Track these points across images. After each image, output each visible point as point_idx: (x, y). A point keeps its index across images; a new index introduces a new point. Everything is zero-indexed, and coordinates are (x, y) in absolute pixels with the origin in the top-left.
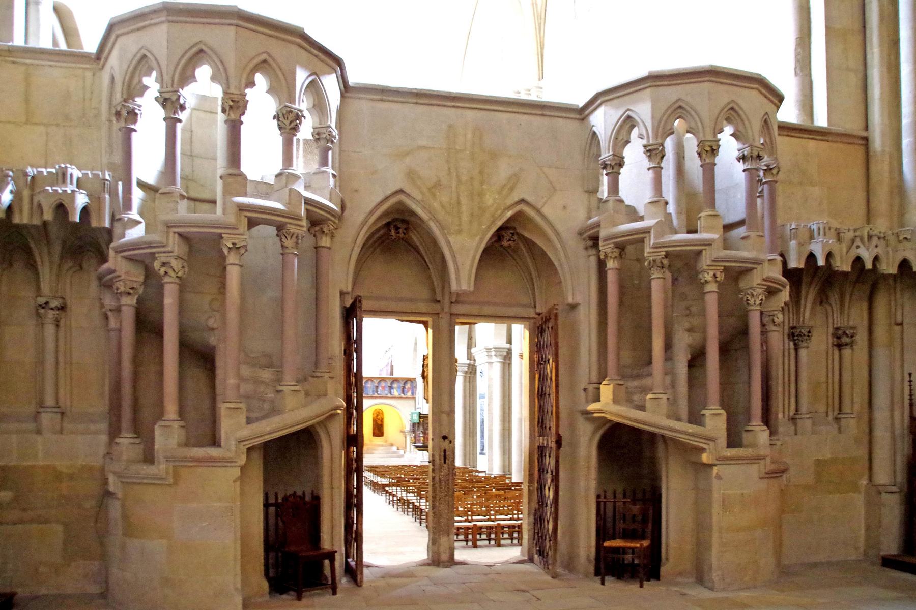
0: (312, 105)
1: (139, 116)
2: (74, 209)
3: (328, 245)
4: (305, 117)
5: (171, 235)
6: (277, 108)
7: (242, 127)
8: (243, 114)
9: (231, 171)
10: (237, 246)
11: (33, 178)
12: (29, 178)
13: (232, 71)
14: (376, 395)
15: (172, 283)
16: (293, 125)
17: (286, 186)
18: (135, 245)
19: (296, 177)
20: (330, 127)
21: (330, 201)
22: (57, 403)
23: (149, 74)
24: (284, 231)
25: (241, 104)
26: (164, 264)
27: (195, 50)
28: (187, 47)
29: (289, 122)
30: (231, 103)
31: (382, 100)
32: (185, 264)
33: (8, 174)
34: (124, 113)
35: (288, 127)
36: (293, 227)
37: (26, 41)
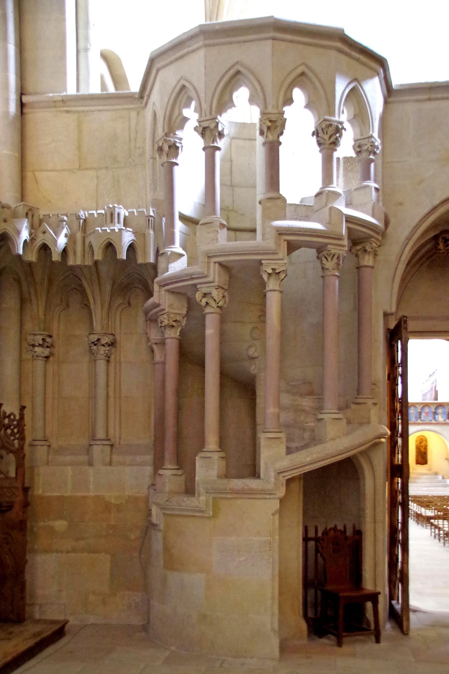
0: (352, 117)
1: (180, 149)
2: (121, 247)
4: (345, 129)
5: (212, 265)
6: (316, 123)
7: (281, 148)
8: (282, 133)
9: (270, 195)
10: (277, 271)
11: (85, 220)
12: (82, 221)
13: (269, 89)
14: (419, 421)
15: (212, 313)
16: (332, 139)
17: (326, 205)
18: (177, 278)
19: (336, 195)
20: (372, 137)
21: (373, 216)
22: (107, 436)
23: (188, 105)
24: (325, 253)
25: (279, 123)
26: (205, 295)
27: (232, 72)
28: (224, 70)
29: (328, 136)
30: (269, 124)
31: (430, 99)
32: (226, 293)
33: (63, 218)
34: (166, 148)
35: (328, 142)
36: (334, 247)
37: (78, 90)
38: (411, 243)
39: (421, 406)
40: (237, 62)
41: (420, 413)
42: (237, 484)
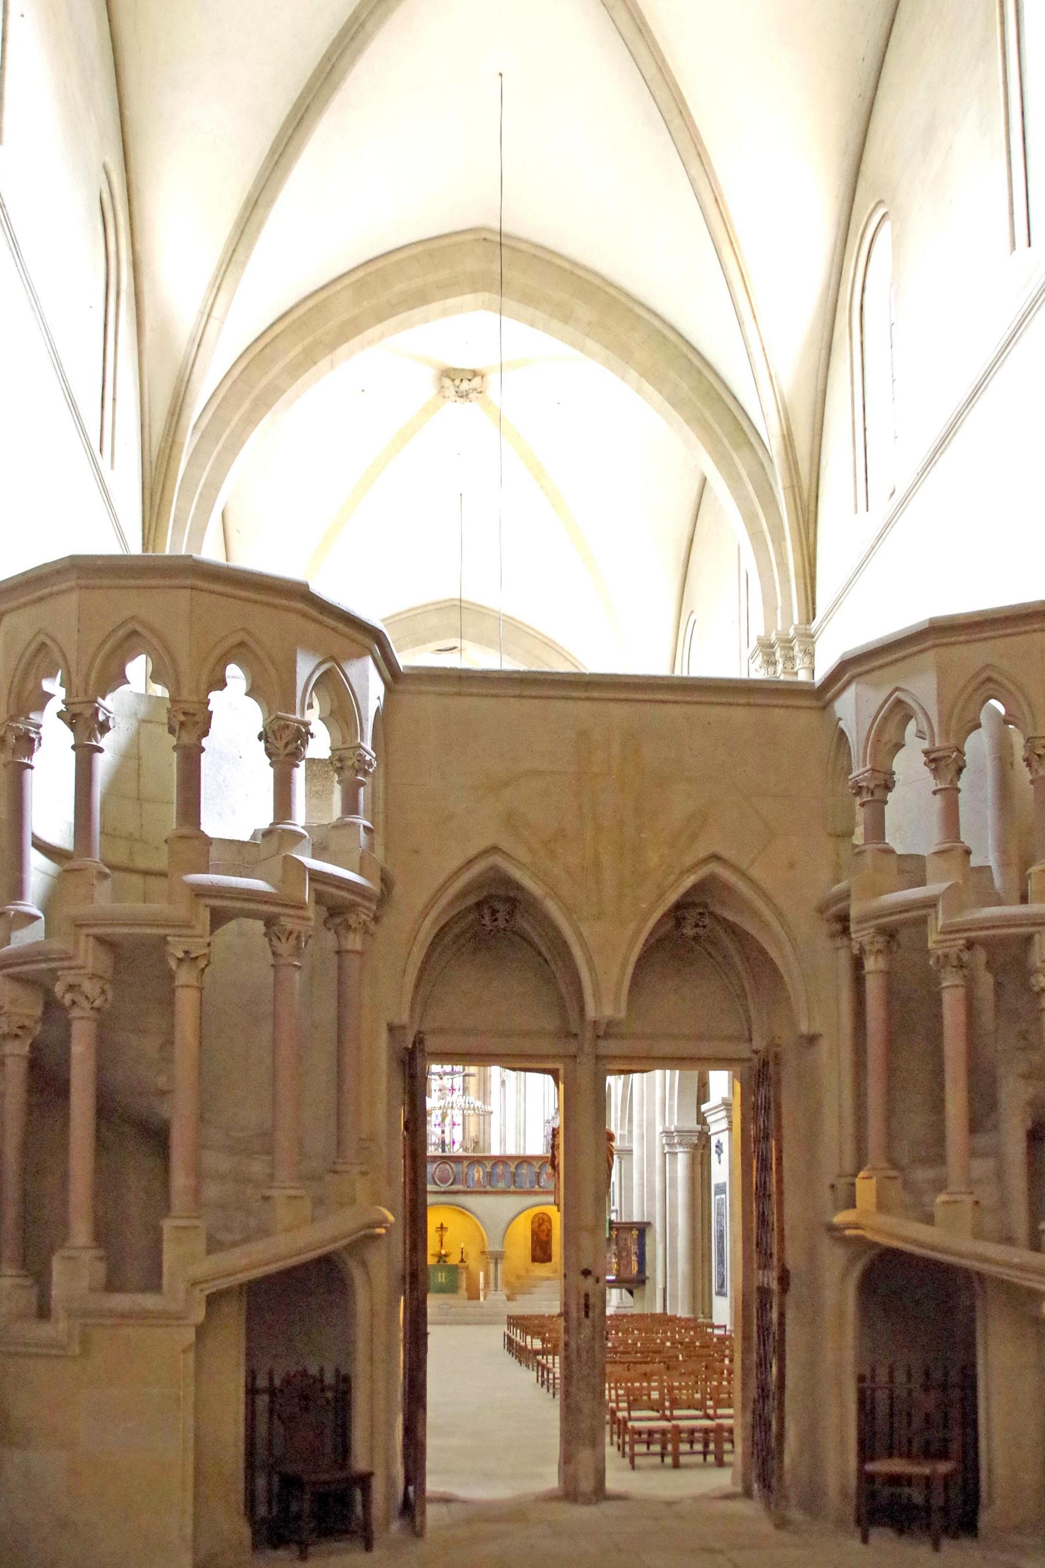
3: (358, 947)
5: (82, 939)
10: (193, 955)
15: (82, 1018)
17: (278, 853)
21: (361, 873)
24: (275, 928)
25: (199, 718)
26: (71, 988)
27: (121, 633)
30: (182, 718)
32: (107, 987)
38: (433, 914)
39: (540, 1163)
40: (133, 618)
41: (538, 1175)
42: (121, 1301)
